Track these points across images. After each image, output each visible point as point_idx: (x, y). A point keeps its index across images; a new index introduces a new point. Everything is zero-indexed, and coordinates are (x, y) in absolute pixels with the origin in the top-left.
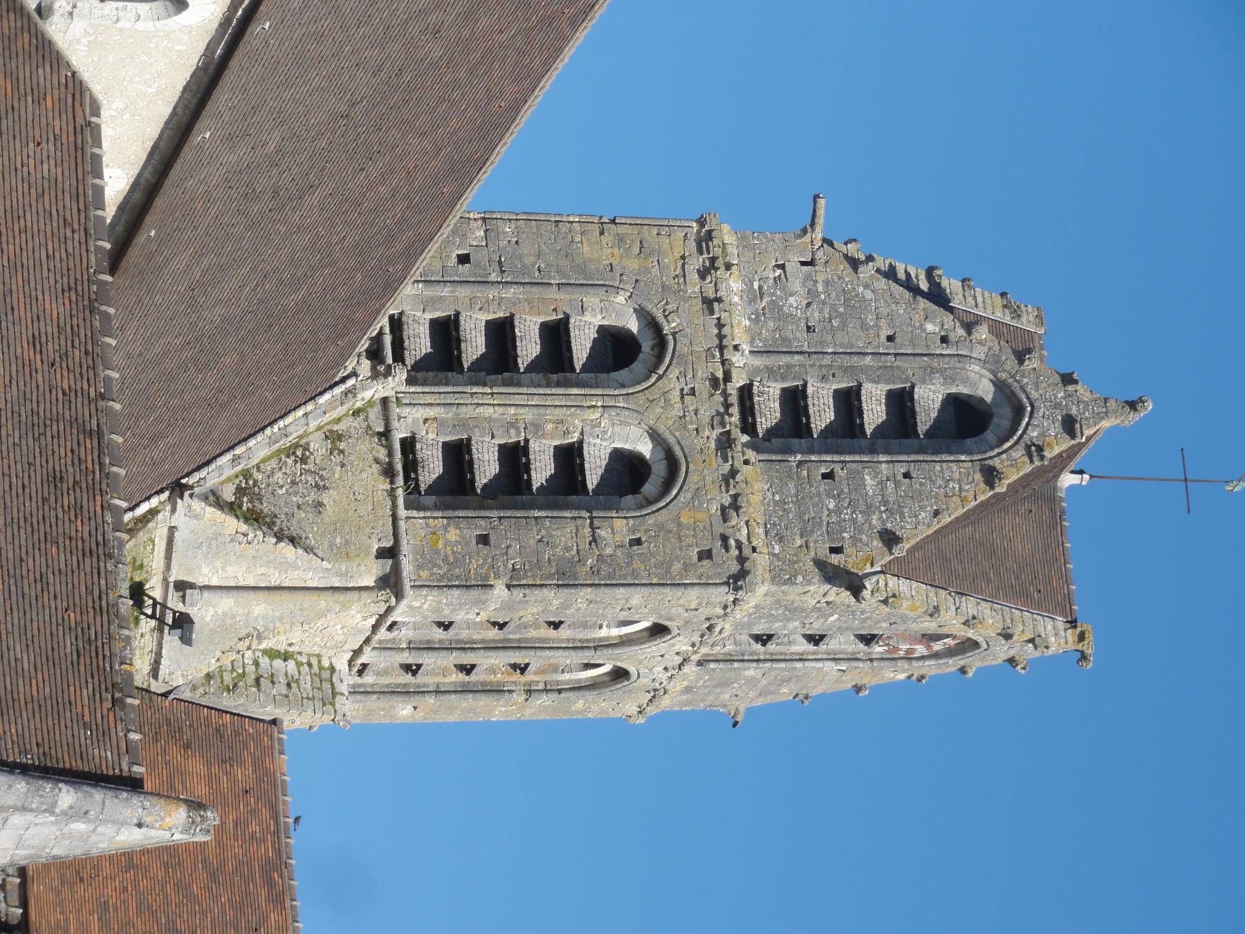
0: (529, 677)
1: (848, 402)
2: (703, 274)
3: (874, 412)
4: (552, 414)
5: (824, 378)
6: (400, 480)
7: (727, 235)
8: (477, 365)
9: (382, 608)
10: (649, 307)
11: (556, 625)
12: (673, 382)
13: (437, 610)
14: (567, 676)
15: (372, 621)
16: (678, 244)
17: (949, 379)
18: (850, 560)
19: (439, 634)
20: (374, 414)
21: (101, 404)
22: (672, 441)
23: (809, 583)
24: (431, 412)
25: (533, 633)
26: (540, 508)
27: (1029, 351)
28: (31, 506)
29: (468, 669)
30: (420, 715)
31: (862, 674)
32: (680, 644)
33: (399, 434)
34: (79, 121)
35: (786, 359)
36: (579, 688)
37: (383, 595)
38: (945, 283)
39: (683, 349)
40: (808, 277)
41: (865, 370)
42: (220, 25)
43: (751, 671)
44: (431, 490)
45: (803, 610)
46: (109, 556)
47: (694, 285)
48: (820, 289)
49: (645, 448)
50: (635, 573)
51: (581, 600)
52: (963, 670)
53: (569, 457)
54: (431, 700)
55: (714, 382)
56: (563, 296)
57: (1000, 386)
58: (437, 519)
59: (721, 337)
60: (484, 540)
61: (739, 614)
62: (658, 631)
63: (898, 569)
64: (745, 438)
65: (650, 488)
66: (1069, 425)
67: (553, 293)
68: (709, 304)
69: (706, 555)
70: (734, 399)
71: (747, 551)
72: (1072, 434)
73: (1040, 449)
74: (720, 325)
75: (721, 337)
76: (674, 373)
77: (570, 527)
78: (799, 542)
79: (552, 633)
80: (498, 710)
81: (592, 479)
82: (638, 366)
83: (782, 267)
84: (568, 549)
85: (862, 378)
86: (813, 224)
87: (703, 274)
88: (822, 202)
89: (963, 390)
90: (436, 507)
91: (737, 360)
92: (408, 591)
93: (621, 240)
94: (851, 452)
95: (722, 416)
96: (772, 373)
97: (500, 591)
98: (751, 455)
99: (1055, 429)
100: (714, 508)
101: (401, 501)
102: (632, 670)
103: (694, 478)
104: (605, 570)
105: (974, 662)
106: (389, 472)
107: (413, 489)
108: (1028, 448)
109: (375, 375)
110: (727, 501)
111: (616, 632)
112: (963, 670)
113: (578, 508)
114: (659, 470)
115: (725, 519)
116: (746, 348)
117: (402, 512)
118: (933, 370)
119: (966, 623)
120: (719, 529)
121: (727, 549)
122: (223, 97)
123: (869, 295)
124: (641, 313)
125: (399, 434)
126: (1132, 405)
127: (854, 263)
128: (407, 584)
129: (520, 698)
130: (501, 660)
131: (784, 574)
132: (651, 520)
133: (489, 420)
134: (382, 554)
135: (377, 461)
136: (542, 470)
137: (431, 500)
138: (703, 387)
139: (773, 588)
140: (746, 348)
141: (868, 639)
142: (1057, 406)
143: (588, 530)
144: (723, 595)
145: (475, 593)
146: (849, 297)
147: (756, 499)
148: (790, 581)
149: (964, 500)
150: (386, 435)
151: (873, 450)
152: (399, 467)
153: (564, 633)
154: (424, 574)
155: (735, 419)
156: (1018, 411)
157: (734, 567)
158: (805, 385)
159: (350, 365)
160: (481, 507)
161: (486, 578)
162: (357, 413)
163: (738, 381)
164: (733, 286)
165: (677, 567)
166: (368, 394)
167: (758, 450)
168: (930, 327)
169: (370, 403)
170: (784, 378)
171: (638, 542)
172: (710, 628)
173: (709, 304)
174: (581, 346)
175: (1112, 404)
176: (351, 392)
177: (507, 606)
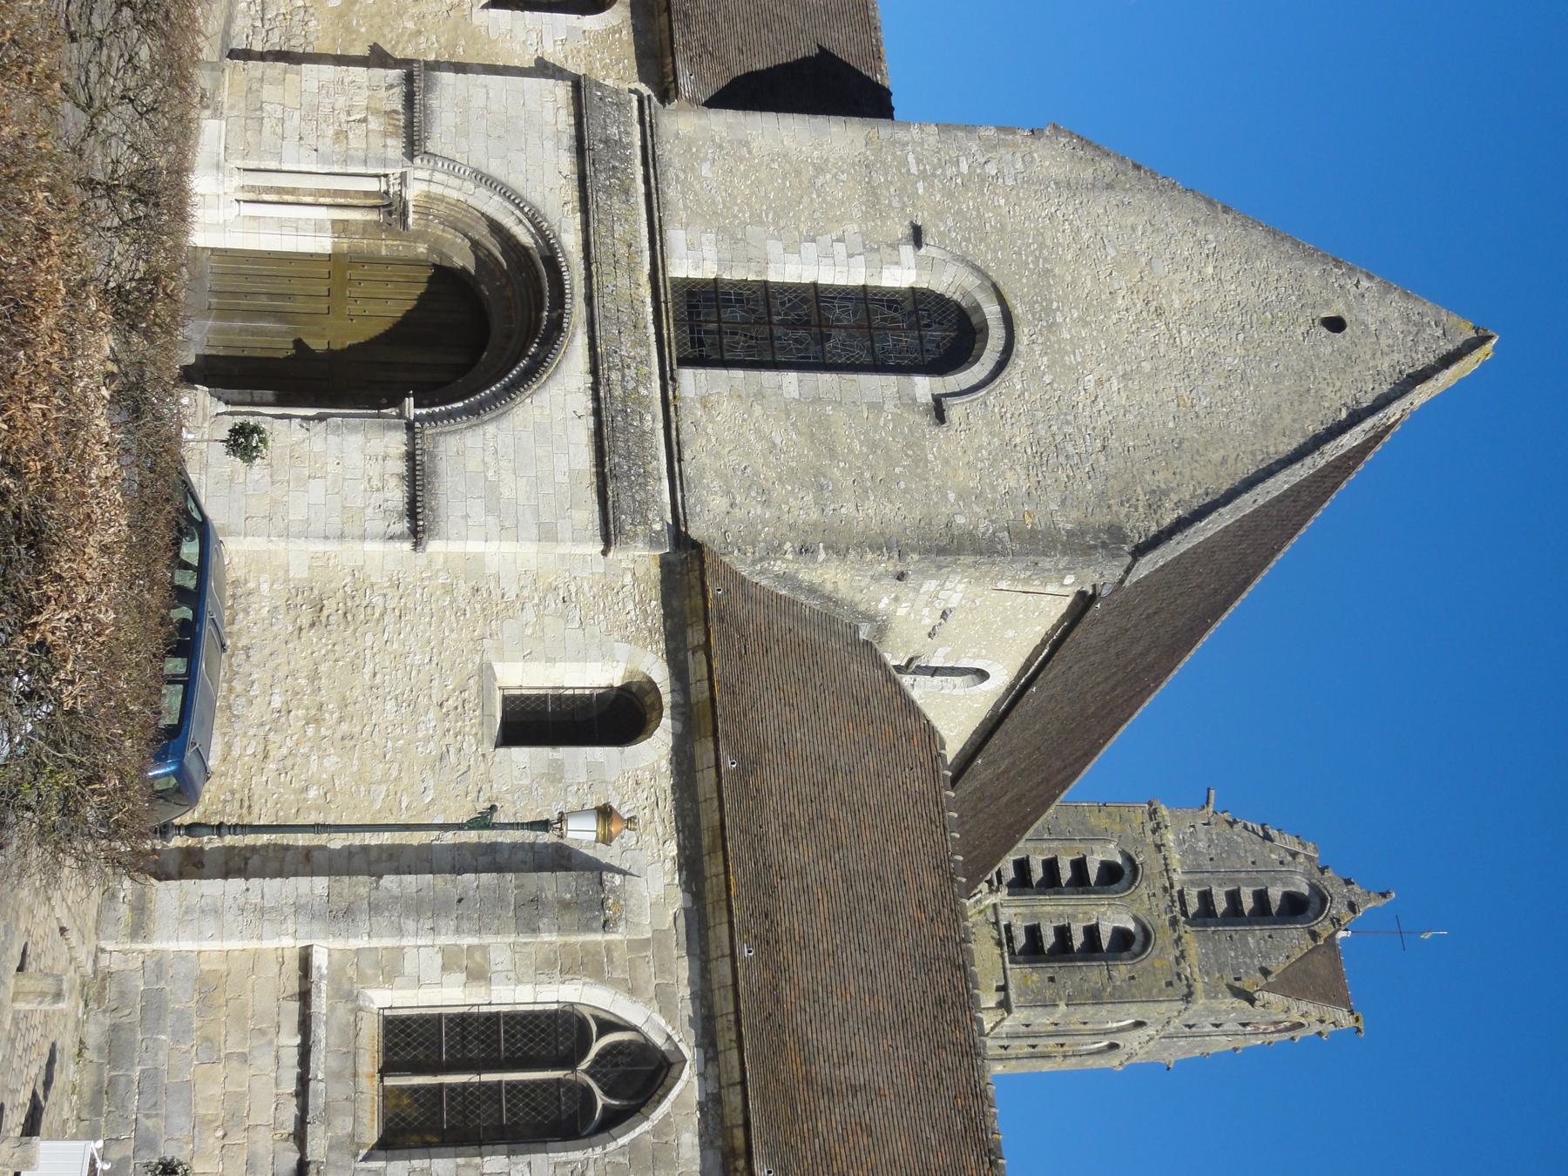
0: (1065, 1048)
1: (1234, 898)
2: (1154, 831)
3: (1248, 903)
4: (1081, 909)
5: (1220, 885)
6: (1006, 948)
7: (1164, 811)
8: (1040, 884)
9: (999, 1018)
10: (1127, 850)
11: (1085, 1023)
12: (1143, 889)
13: (1027, 1019)
14: (1085, 1047)
15: (992, 1025)
16: (1139, 815)
17: (1285, 884)
18: (1247, 984)
19: (1024, 1029)
20: (989, 912)
21: (964, 945)
22: (1146, 922)
23: (1225, 998)
24: (1018, 910)
25: (1072, 1027)
26: (1080, 961)
27: (1327, 867)
28: (927, 1022)
29: (1034, 1047)
30: (1006, 1071)
31: (1240, 1042)
32: (1151, 1031)
33: (1003, 923)
34: (934, 753)
35: (1198, 876)
36: (1090, 1054)
37: (1000, 1012)
38: (1271, 832)
39: (1147, 872)
40: (1207, 832)
41: (1240, 880)
42: (1007, 690)
43: (1182, 1042)
44: (1021, 953)
45: (1218, 1011)
46: (978, 1054)
47: (1150, 838)
48: (1214, 837)
49: (1131, 926)
50: (1133, 996)
51: (1104, 1011)
52: (1293, 1039)
53: (1092, 932)
54: (1013, 1062)
55: (1165, 890)
56: (1082, 845)
57: (1312, 886)
58: (1026, 969)
59: (1166, 865)
60: (1052, 979)
61: (1186, 1015)
62: (1139, 1024)
63: (1270, 988)
64: (1183, 919)
65: (1136, 947)
66: (1352, 907)
67: (1077, 845)
68: (1159, 847)
69: (1169, 984)
70: (1176, 898)
71: (1191, 982)
72: (1354, 912)
73: (1338, 920)
74: (1165, 859)
75: (1166, 865)
76: (1144, 884)
77: (1096, 972)
78: (1217, 975)
79: (1082, 1026)
80: (1047, 1066)
81: (1105, 945)
82: (1124, 882)
83: (1193, 826)
84: (1097, 983)
85: (1240, 883)
86: (1208, 803)
87: (1154, 831)
88: (1212, 792)
89: (1293, 889)
90: (1025, 962)
91: (1175, 877)
92: (1014, 1010)
93: (1110, 814)
94: (1239, 925)
95: (1170, 908)
96: (1193, 883)
97: (1062, 1007)
98: (1188, 928)
99: (1344, 910)
100: (1172, 958)
101: (1007, 960)
102: (1122, 1044)
103: (1159, 942)
104: (1117, 994)
105: (1299, 1034)
106: (999, 944)
107: (1012, 953)
108: (1332, 920)
109: (991, 891)
110: (1178, 954)
111: (1115, 1025)
112: (1293, 1039)
113: (1100, 960)
114: (1139, 938)
115: (1178, 964)
116: (1179, 870)
117: (1008, 965)
118: (1277, 879)
119: (1302, 1016)
120: (1175, 969)
121: (1180, 979)
122: (996, 739)
123: (1240, 840)
124: (1123, 853)
125: (1003, 923)
126: (1384, 895)
127: (1231, 824)
128: (1013, 1005)
129: (1059, 1060)
130: (1052, 1041)
131: (1212, 993)
132: (1139, 966)
133: (1049, 913)
134: (999, 989)
135: (993, 938)
136: (1078, 940)
137: (1021, 958)
138: (1159, 892)
139: (1206, 1001)
140: (1179, 870)
141: (1244, 1025)
142: (1344, 896)
143: (1106, 972)
144: (1181, 1005)
145: (1049, 1009)
146: (1229, 841)
147: (1193, 952)
148: (1215, 997)
149: (1302, 949)
150: (996, 923)
151: (1250, 924)
152: (1005, 941)
153: (1089, 1026)
154: (1022, 999)
155: (1178, 909)
156: (1323, 900)
157: (1185, 990)
158: (1211, 890)
159: (980, 887)
160: (1048, 962)
161: (1055, 1001)
162: (980, 912)
163: (1177, 888)
164: (1170, 837)
165: (1155, 991)
166: (987, 902)
167: (1192, 926)
168: (1273, 856)
169: (987, 907)
170: (1199, 886)
171: (1133, 978)
172: (1168, 1023)
173: (1159, 847)
174: (1093, 873)
175: (1372, 894)
176: (979, 901)
177: (1065, 1015)
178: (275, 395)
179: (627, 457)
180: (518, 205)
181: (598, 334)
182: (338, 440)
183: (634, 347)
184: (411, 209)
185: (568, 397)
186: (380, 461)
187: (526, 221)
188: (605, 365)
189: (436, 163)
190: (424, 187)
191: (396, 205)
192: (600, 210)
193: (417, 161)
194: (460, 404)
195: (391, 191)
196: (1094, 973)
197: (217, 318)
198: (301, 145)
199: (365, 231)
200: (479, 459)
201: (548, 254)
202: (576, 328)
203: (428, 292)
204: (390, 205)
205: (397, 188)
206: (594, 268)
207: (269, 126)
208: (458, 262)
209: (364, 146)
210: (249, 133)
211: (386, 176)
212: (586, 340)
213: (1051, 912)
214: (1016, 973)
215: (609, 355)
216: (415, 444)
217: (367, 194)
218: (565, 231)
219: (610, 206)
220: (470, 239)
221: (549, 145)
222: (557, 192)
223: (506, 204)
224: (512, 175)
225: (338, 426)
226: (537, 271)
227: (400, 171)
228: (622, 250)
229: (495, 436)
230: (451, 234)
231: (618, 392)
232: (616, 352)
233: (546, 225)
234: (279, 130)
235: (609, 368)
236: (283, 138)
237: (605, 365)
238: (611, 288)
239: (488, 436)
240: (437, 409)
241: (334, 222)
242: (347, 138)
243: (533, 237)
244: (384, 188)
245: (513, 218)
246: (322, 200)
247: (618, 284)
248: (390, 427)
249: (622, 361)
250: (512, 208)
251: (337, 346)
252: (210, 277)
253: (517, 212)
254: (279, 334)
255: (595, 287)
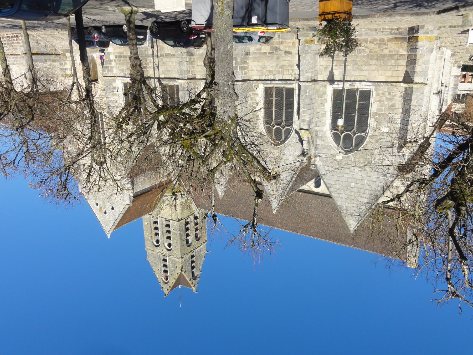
7: (206, 243)
17: (196, 271)
49: (190, 243)
57: (196, 277)
96: (195, 253)
99: (194, 284)
126: (196, 291)
196: (184, 237)
213: (191, 226)
214: (183, 221)
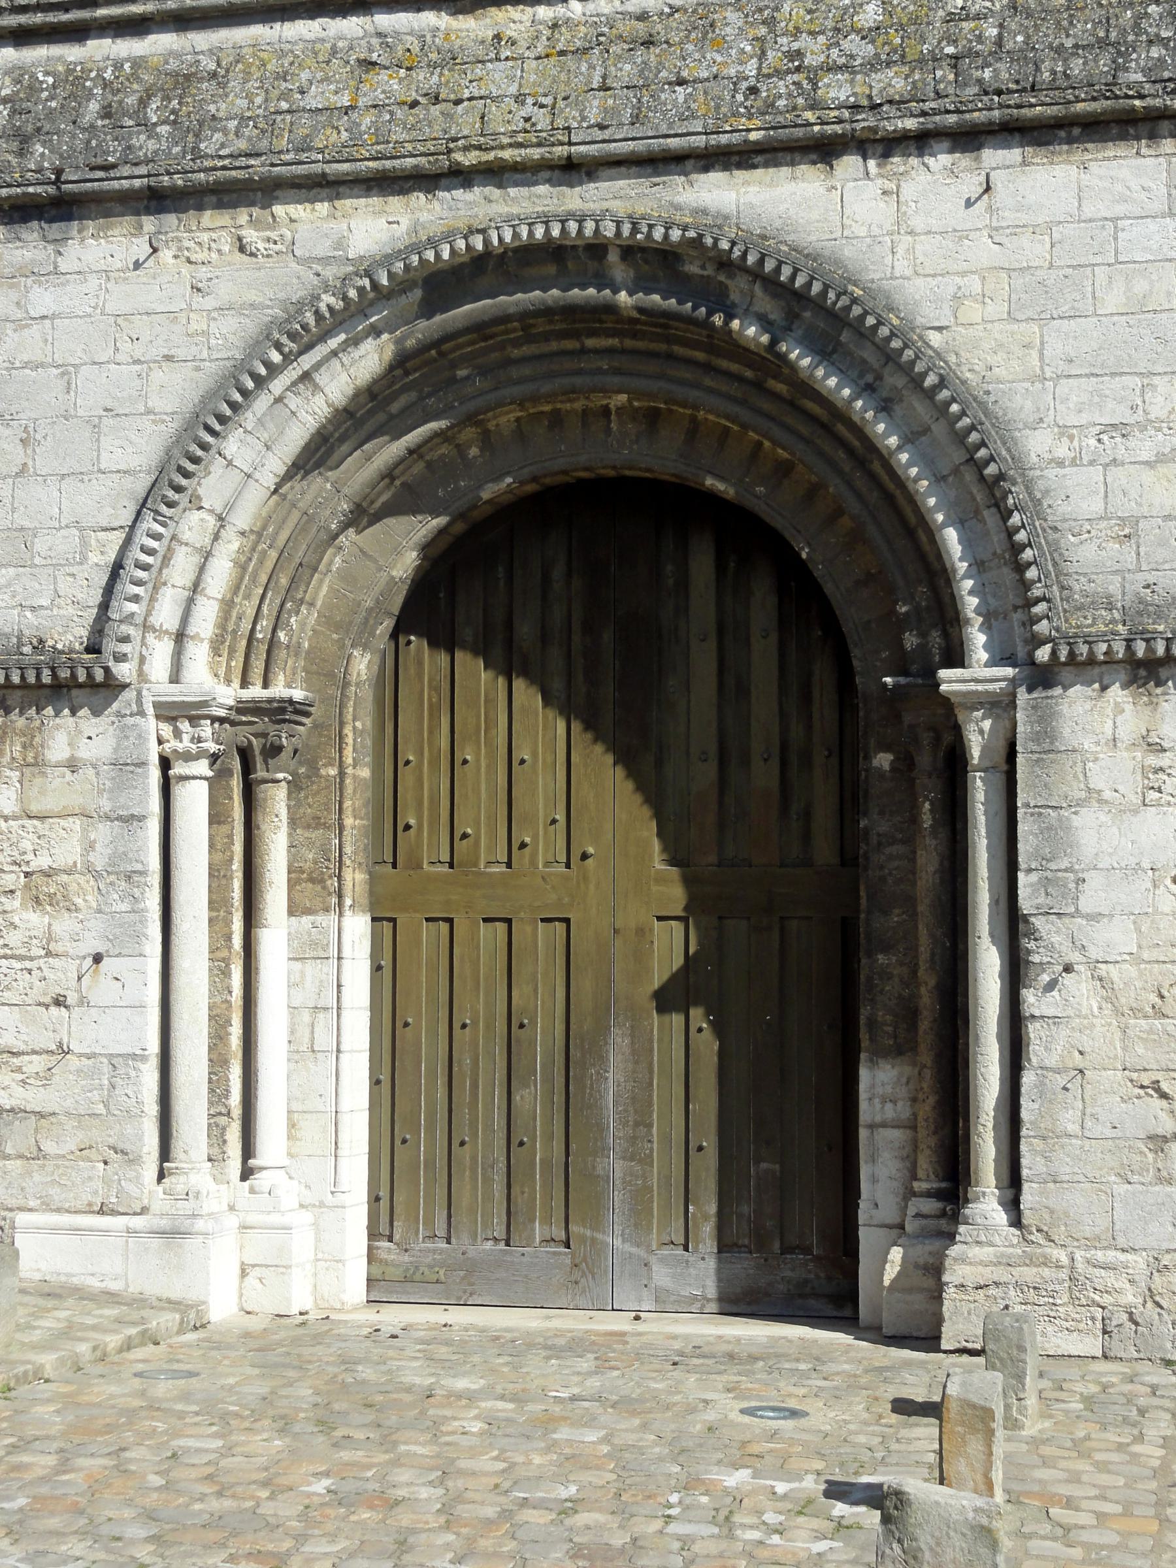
178: (873, 1063)
179: (1121, 51)
180: (260, 381)
181: (699, 141)
182: (1094, 881)
183: (721, 44)
184: (255, 692)
185: (918, 223)
186: (1164, 760)
187: (307, 361)
188: (809, 116)
189: (129, 618)
190: (198, 656)
191: (243, 735)
192: (264, 144)
193: (124, 671)
194: (951, 536)
195: (213, 747)
197: (597, 1223)
198: (83, 1001)
199: (317, 823)
200: (1147, 476)
201: (418, 293)
202: (678, 207)
203: (482, 649)
204: (245, 754)
205: (206, 730)
206: (468, 159)
207: (19, 1091)
208: (405, 564)
209: (76, 824)
210: (49, 1147)
211: (165, 764)
212: (716, 177)
215: (769, 106)
216: (1110, 660)
217: (217, 817)
218: (340, 244)
219: (244, 120)
220: (344, 527)
221: (43, 299)
222: (203, 272)
223: (249, 418)
224: (155, 402)
225: (1046, 883)
226: (480, 329)
227: (151, 724)
228: (388, 84)
229: (1064, 431)
230: (321, 581)
231: (894, 81)
232: (753, 90)
233: (328, 299)
234: (36, 1064)
235: (812, 108)
236: (64, 1051)
237: (809, 116)
238: (528, 109)
239: (1062, 451)
240: (972, 602)
241: (294, 910)
242: (48, 874)
243: (355, 341)
244: (202, 767)
245: (293, 401)
246: (237, 941)
247: (513, 89)
248: (1046, 734)
249: (778, 73)
250: (262, 403)
251: (675, 896)
252: (461, 1241)
253: (278, 385)
254: (640, 1053)
255: (536, 153)
